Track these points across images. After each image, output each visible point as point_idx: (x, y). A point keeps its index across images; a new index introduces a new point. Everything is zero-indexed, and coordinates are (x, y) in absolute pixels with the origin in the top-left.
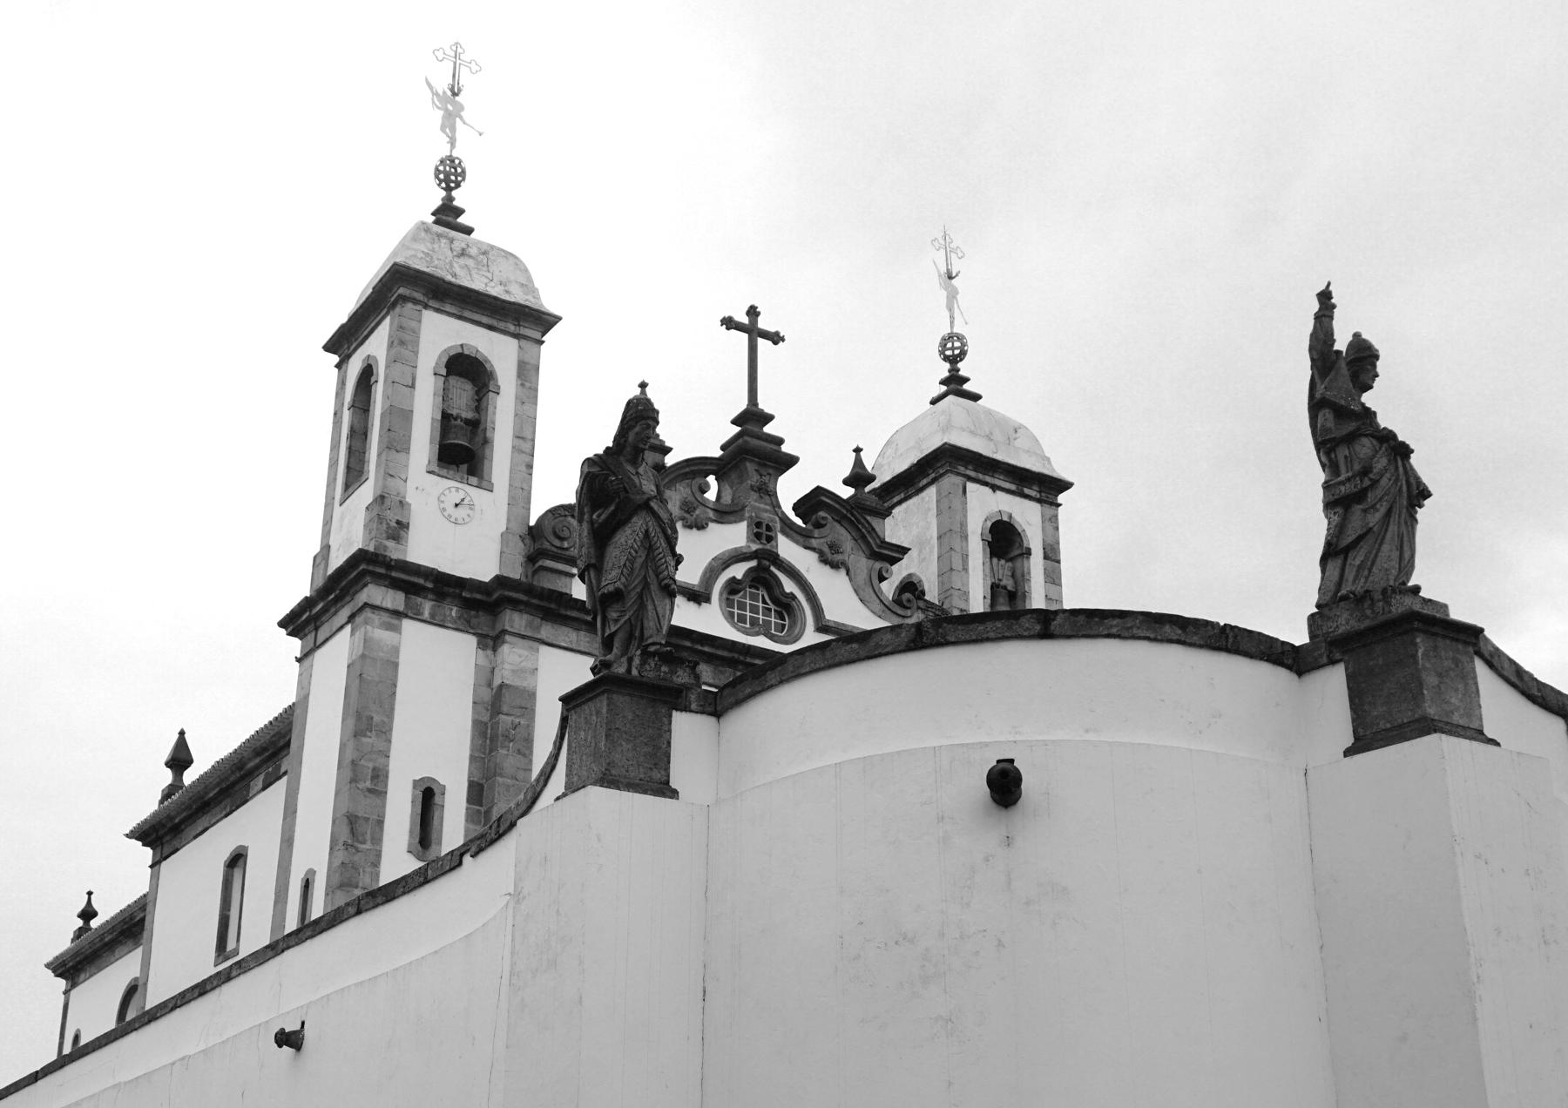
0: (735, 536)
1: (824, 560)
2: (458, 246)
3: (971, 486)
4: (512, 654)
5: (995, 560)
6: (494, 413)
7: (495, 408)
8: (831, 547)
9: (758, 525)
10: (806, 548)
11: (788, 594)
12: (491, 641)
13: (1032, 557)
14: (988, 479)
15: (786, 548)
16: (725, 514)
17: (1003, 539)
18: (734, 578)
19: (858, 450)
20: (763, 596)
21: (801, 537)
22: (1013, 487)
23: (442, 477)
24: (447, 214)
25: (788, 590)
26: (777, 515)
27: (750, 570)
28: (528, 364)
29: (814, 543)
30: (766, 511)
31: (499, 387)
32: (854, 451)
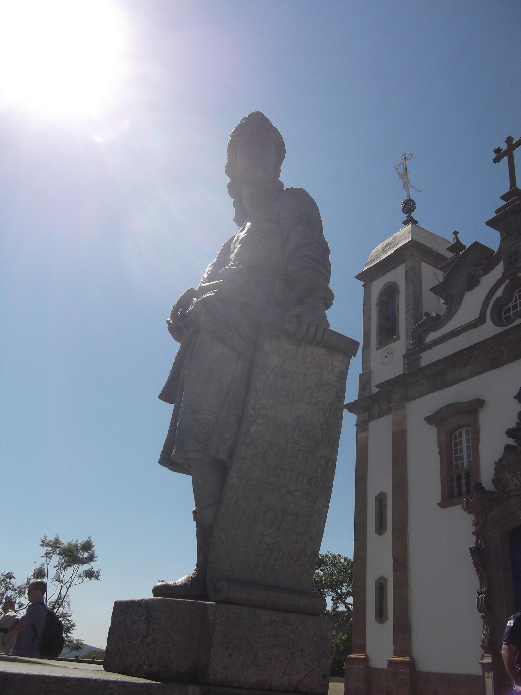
6: (398, 304)
7: (398, 300)
18: (498, 298)
27: (508, 285)
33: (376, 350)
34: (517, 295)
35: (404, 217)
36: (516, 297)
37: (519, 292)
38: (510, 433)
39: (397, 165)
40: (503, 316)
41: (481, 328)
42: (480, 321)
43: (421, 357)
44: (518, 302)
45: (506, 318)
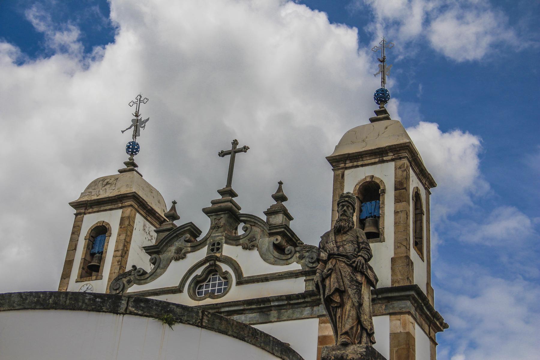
0: (203, 253)
1: (245, 248)
2: (105, 183)
3: (347, 172)
5: (368, 203)
6: (107, 245)
7: (108, 242)
8: (249, 240)
9: (214, 245)
10: (237, 245)
11: (224, 272)
13: (386, 196)
14: (360, 163)
15: (228, 250)
16: (196, 247)
18: (197, 275)
19: (280, 183)
20: (219, 277)
22: (377, 160)
23: (82, 282)
24: (131, 166)
25: (224, 271)
26: (224, 236)
27: (207, 268)
28: (124, 217)
31: (111, 234)
32: (173, 202)
33: (76, 282)
34: (211, 277)
35: (127, 157)
36: (210, 278)
37: (212, 276)
39: (131, 103)
40: (197, 291)
41: (177, 295)
42: (178, 290)
44: (211, 283)
45: (198, 292)
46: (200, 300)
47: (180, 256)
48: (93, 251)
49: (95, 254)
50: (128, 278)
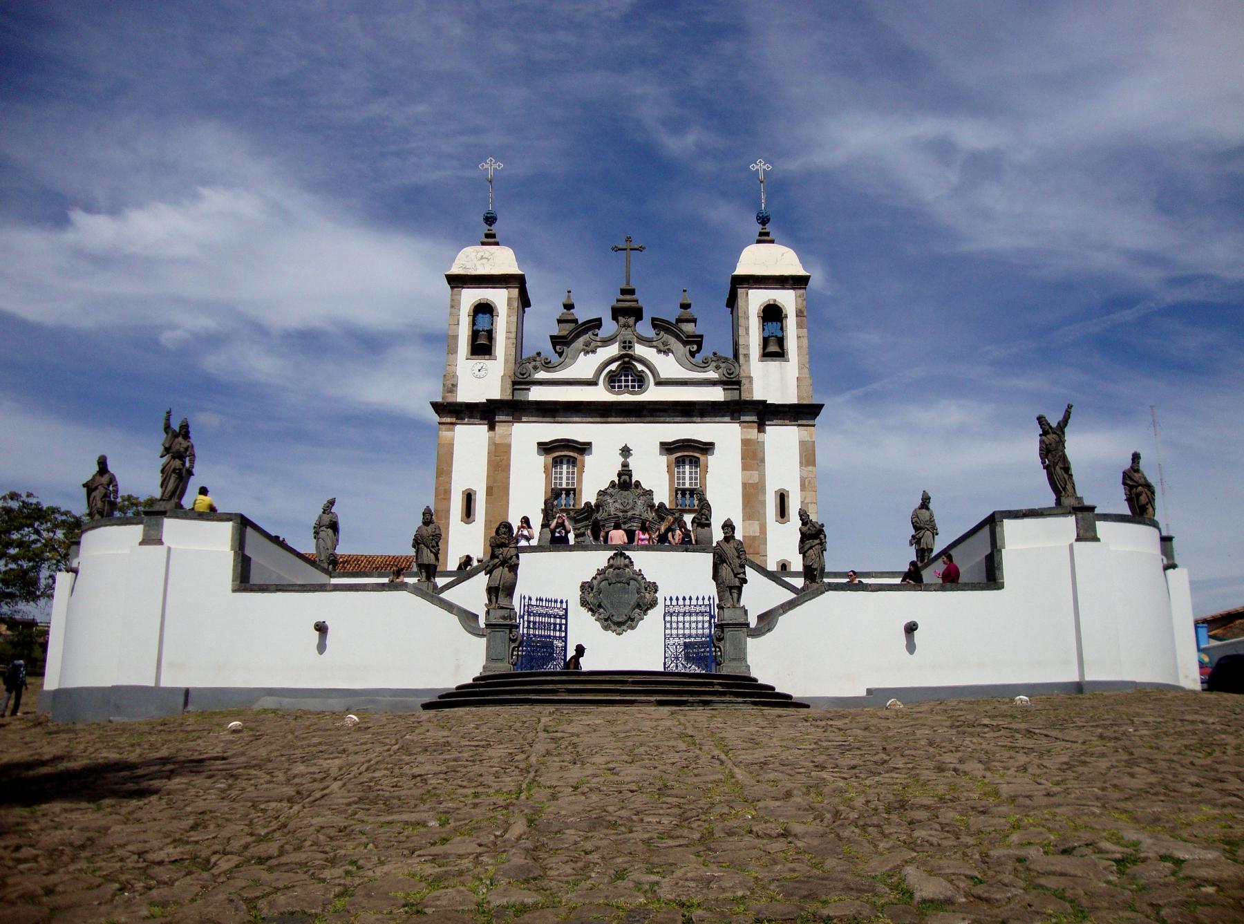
1: (659, 351)
2: (479, 255)
3: (750, 291)
4: (500, 429)
9: (625, 342)
10: (650, 347)
12: (492, 427)
15: (640, 350)
16: (606, 342)
17: (772, 314)
18: (611, 371)
21: (647, 342)
29: (654, 344)
30: (628, 334)
38: (620, 475)
43: (529, 389)
46: (618, 393)
47: (589, 350)
48: (475, 328)
49: (479, 331)
50: (533, 364)
